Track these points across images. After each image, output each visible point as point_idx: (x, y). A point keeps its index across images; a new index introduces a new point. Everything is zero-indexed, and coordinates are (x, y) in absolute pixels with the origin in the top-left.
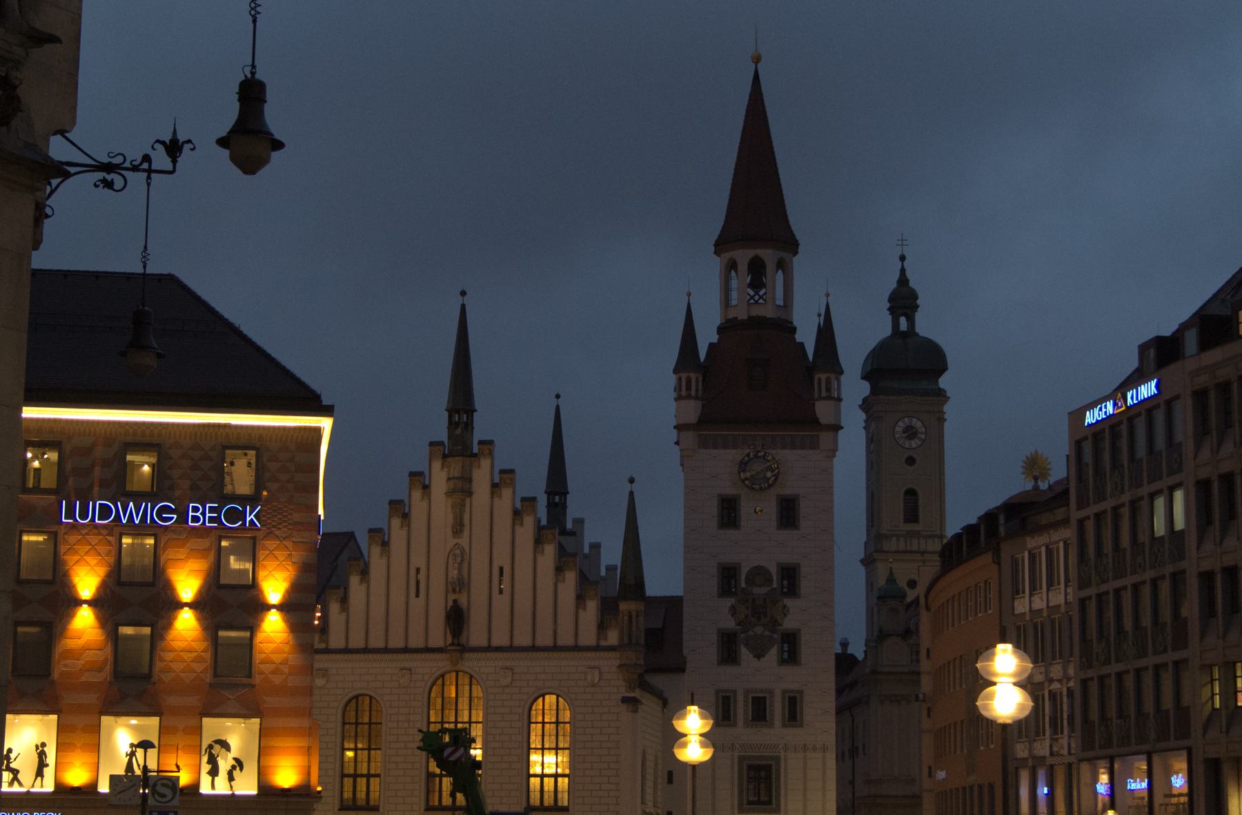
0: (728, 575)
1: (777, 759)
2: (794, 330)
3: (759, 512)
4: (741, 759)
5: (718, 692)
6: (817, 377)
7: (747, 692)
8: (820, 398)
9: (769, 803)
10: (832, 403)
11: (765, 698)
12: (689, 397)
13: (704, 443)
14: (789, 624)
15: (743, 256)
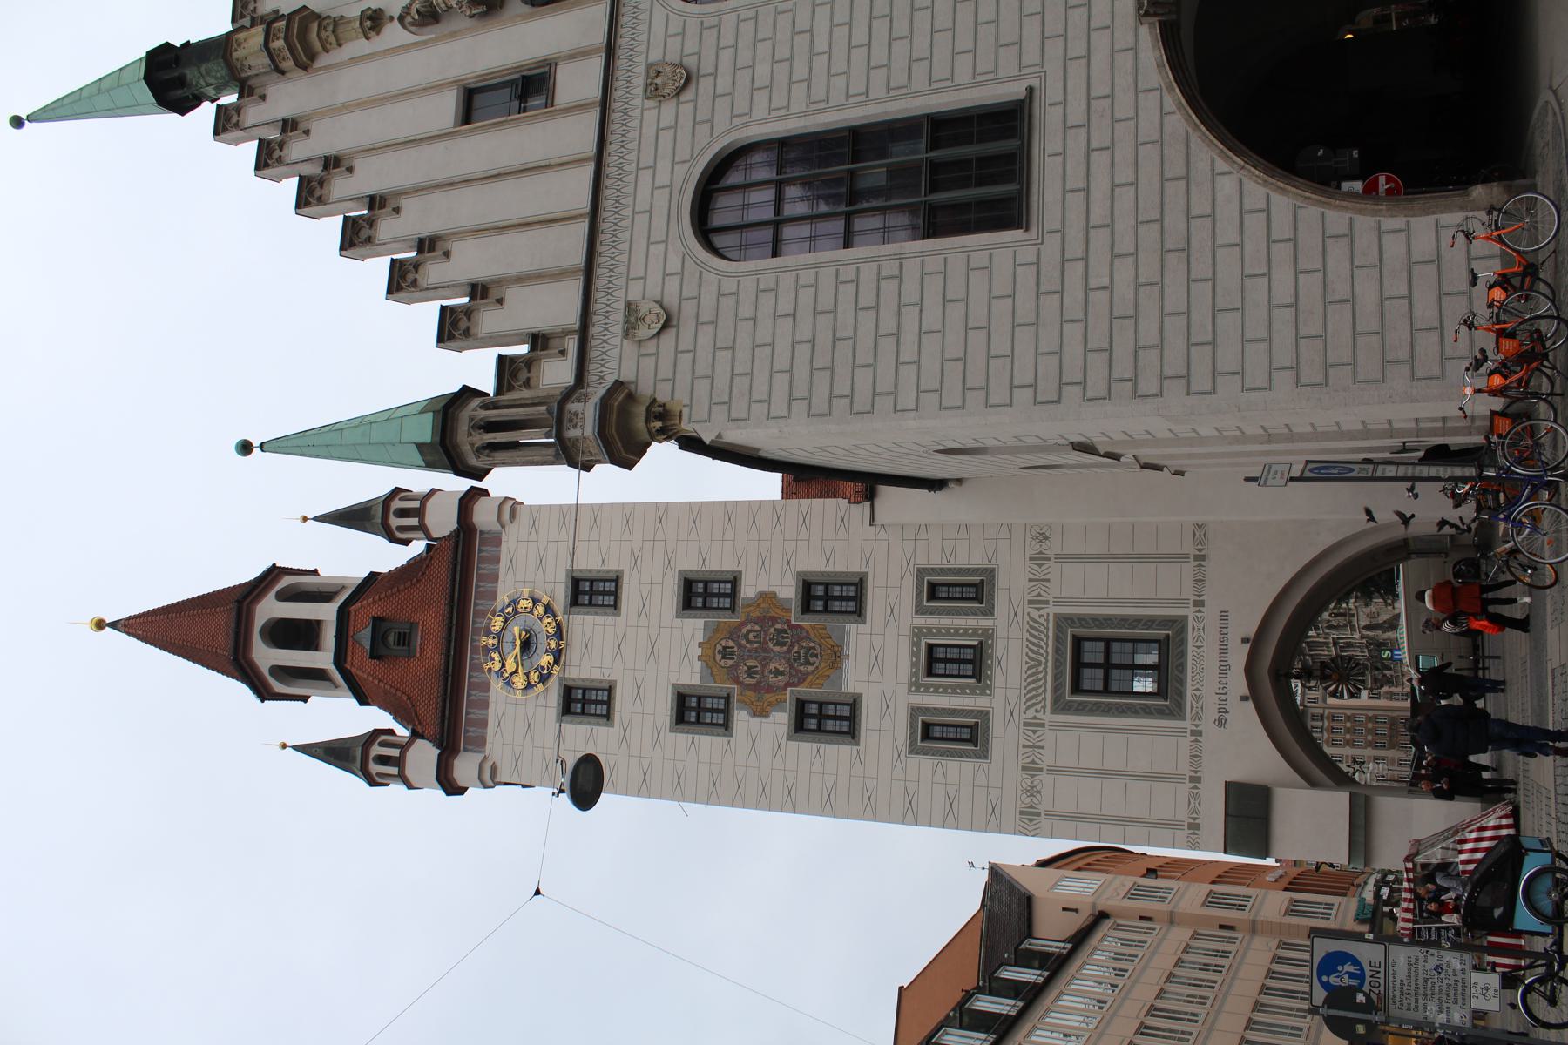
0: (691, 711)
1: (1062, 621)
2: (373, 576)
3: (595, 647)
4: (1060, 706)
5: (913, 749)
6: (400, 535)
7: (916, 687)
8: (422, 528)
9: (1163, 645)
10: (430, 504)
11: (931, 647)
12: (399, 762)
13: (480, 743)
14: (789, 592)
15: (266, 656)
